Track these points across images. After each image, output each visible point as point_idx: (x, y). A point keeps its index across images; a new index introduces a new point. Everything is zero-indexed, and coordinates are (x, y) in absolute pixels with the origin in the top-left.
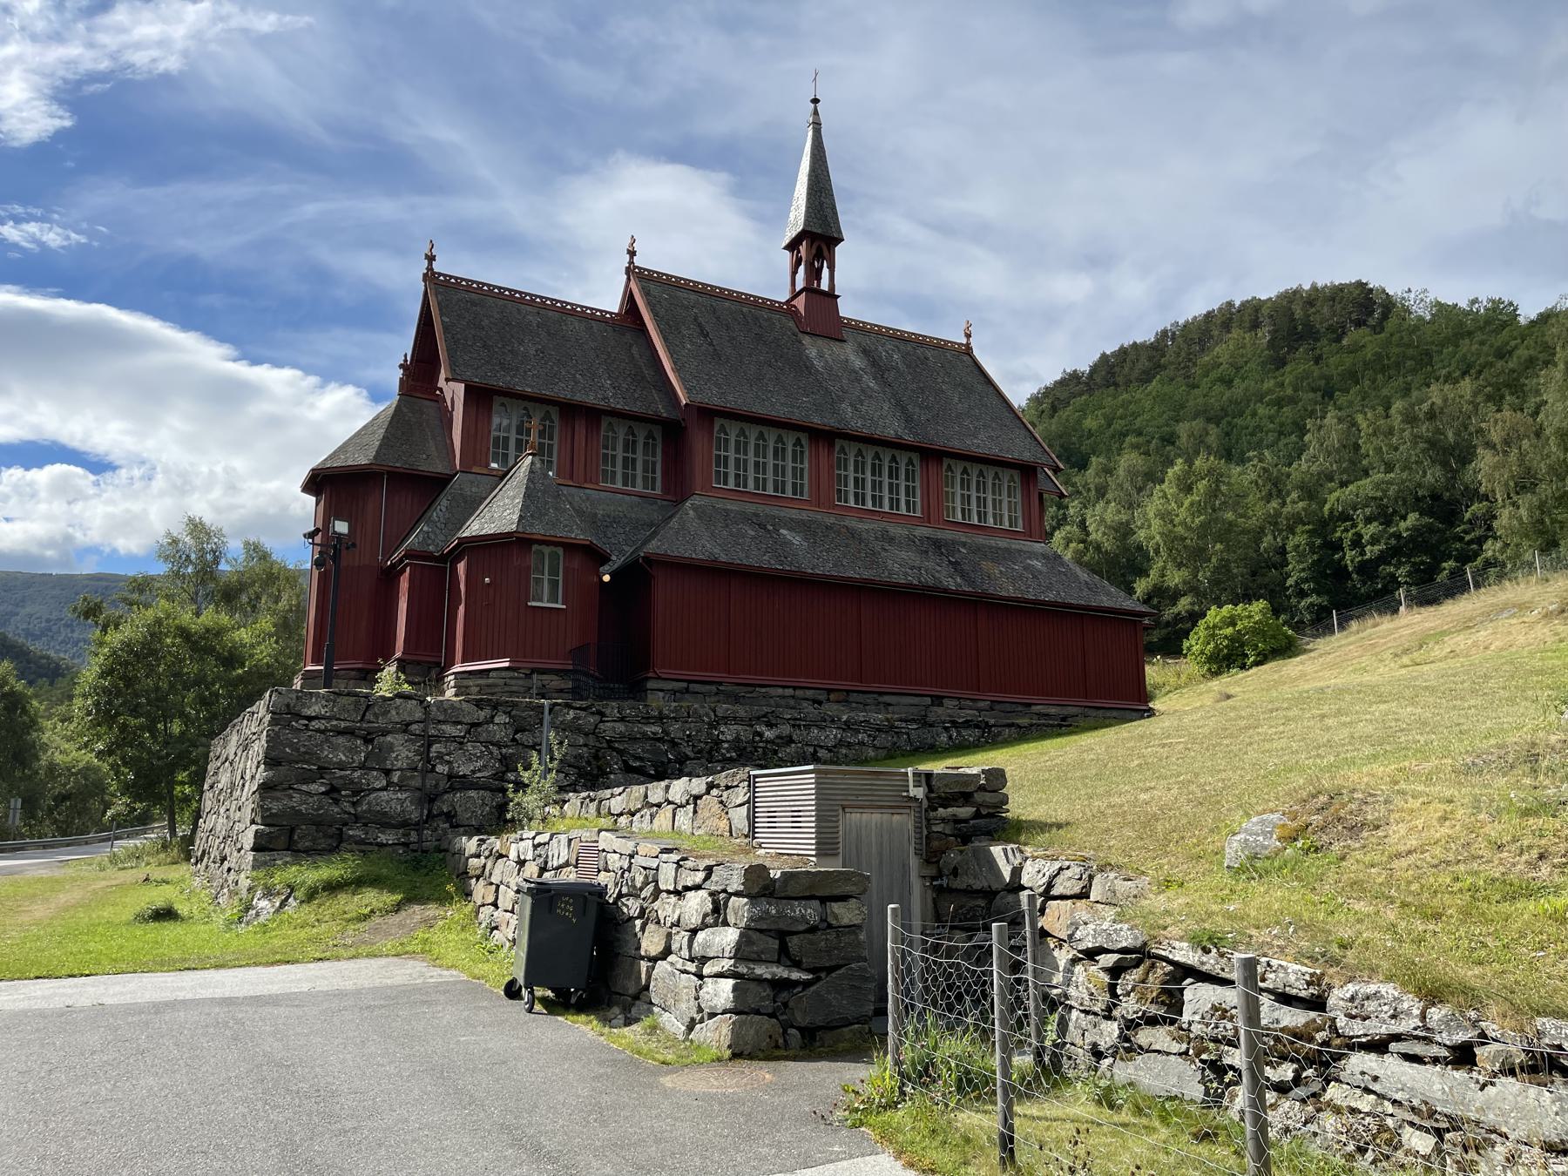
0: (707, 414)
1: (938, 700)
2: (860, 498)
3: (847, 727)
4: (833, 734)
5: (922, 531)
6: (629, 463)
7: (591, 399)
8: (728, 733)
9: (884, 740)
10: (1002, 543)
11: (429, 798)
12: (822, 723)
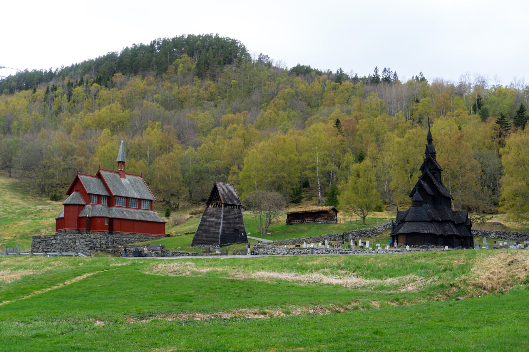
0: (115, 196)
1: (141, 234)
2: (131, 206)
3: (135, 238)
4: (133, 239)
5: (139, 211)
6: (103, 202)
7: (100, 194)
8: (124, 239)
9: (138, 240)
10: (148, 211)
11: (101, 245)
12: (132, 238)
